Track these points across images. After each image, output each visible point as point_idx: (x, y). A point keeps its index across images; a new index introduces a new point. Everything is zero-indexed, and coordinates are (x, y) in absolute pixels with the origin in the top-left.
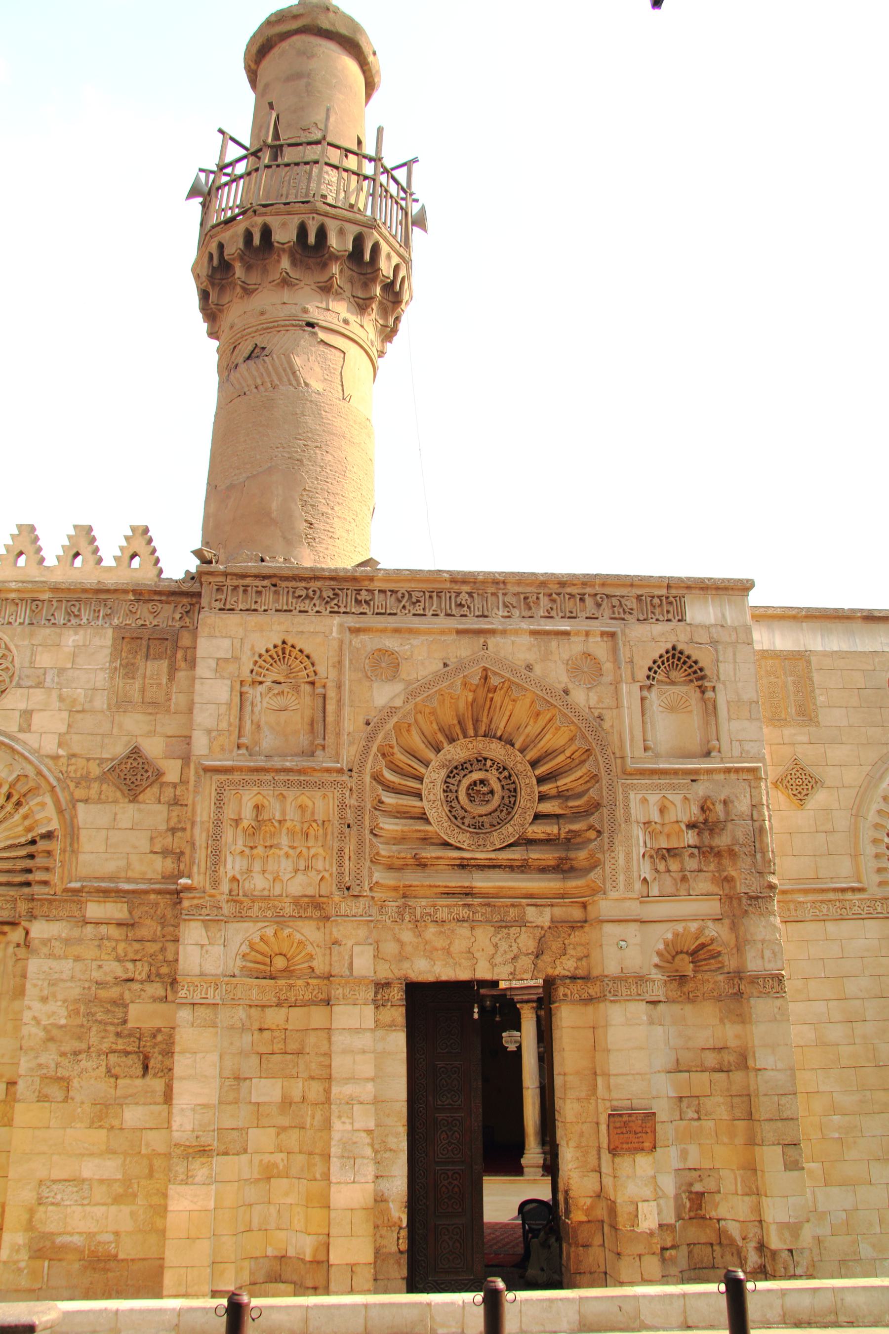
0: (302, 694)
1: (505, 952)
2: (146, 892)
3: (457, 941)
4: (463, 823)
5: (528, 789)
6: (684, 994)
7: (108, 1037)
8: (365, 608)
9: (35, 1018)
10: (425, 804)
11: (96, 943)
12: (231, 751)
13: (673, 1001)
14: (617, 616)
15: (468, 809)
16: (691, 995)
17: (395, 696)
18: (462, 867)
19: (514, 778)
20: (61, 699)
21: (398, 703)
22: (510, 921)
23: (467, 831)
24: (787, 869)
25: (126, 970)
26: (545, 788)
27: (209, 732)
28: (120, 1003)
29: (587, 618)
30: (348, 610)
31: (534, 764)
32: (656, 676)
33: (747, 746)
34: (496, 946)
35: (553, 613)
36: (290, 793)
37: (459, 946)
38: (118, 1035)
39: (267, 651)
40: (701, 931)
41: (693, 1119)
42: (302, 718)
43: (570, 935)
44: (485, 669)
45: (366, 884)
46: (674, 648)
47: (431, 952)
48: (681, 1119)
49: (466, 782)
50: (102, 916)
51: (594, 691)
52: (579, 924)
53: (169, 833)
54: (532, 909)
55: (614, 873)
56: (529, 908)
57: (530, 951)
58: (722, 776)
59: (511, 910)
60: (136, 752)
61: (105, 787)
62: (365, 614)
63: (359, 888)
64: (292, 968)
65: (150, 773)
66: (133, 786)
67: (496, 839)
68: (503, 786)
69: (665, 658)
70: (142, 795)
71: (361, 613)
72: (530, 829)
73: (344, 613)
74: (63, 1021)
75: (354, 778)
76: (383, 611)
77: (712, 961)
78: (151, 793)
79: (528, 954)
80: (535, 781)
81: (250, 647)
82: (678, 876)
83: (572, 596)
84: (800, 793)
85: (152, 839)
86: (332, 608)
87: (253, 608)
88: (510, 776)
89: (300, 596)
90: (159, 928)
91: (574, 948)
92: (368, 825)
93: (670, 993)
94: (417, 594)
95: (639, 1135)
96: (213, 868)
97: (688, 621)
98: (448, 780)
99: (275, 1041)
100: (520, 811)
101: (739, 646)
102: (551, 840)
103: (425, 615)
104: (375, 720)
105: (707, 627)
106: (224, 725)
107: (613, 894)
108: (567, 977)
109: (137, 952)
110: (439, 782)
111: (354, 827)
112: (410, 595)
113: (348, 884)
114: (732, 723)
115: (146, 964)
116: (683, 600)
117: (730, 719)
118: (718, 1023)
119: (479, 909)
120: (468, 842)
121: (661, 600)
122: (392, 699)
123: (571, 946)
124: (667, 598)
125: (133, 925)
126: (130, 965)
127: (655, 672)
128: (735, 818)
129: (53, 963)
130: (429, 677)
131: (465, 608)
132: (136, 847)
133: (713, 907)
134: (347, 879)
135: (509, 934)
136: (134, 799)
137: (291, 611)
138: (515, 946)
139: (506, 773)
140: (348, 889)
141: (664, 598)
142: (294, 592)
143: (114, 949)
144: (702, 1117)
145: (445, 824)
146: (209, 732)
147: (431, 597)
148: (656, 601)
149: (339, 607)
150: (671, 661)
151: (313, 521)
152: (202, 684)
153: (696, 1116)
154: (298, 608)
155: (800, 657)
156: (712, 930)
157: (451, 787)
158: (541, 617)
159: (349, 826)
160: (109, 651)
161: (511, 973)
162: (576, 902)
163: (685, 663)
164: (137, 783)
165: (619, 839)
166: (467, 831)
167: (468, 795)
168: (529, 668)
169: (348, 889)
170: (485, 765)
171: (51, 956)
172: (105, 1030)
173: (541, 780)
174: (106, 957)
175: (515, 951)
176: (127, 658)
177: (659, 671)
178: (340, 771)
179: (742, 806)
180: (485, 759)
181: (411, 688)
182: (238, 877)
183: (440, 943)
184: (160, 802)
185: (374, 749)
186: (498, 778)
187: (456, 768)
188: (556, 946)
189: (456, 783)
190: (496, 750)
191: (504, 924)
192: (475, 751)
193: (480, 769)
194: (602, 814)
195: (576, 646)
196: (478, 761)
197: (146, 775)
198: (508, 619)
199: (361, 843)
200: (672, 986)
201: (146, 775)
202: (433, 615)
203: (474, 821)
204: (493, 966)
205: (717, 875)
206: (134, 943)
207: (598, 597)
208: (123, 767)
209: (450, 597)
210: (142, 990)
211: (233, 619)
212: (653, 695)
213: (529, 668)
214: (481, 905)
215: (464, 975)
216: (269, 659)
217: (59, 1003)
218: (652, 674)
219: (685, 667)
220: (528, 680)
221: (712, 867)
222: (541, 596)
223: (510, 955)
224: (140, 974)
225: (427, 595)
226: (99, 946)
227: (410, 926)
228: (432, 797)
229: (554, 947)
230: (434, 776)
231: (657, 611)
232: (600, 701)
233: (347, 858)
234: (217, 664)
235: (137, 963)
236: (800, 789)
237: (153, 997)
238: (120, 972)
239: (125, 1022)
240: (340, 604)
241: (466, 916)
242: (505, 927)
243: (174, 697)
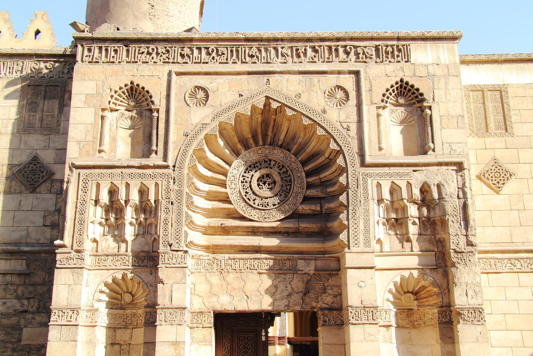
0: (144, 118)
2: (39, 252)
3: (249, 284)
4: (254, 203)
5: (300, 180)
6: (411, 322)
7: (6, 352)
8: (186, 59)
10: (228, 190)
11: (3, 287)
12: (94, 155)
13: (403, 327)
14: (361, 60)
15: (258, 193)
16: (416, 323)
17: (206, 117)
19: (290, 172)
21: (207, 121)
22: (286, 270)
23: (257, 209)
24: (484, 234)
25: (23, 305)
26: (311, 180)
27: (79, 142)
28: (17, 328)
29: (340, 62)
30: (175, 61)
31: (304, 163)
32: (389, 100)
33: (454, 147)
35: (316, 59)
36: (132, 182)
38: (14, 350)
39: (121, 88)
42: (144, 133)
43: (328, 280)
44: (267, 98)
45: (183, 241)
46: (402, 80)
50: (8, 268)
51: (343, 111)
52: (334, 272)
53: (56, 213)
54: (302, 261)
55: (356, 234)
56: (300, 261)
57: (300, 291)
58: (436, 168)
59: (287, 262)
60: (35, 159)
61: (13, 183)
62: (187, 63)
63: (177, 245)
64: (135, 302)
65: (44, 174)
66: (32, 182)
68: (282, 178)
69: (395, 88)
70: (38, 188)
71: (184, 63)
72: (300, 208)
73: (173, 63)
75: (176, 171)
76: (199, 61)
77: (431, 298)
78: (44, 187)
79: (299, 292)
81: (108, 87)
83: (330, 48)
84: (498, 183)
85: (45, 217)
86: (164, 59)
87: (111, 61)
88: (287, 171)
89: (143, 53)
90: (47, 276)
91: (332, 289)
92: (185, 203)
93: (400, 322)
94: (222, 49)
96: (79, 233)
97: (412, 62)
98: (245, 174)
99: (122, 352)
100: (294, 195)
101: (450, 78)
102: (316, 214)
103: (227, 63)
104: (192, 133)
105: (427, 66)
106: (90, 138)
107: (353, 249)
108: (325, 309)
109: (31, 293)
111: (176, 204)
112: (217, 51)
113: (170, 243)
114: (443, 130)
115: (37, 301)
116: (409, 47)
117: (442, 128)
118: (435, 343)
119: (265, 261)
120: (257, 215)
121: (393, 49)
122: (203, 119)
123: (329, 287)
124: (398, 46)
125: (29, 274)
126: (25, 302)
127: (388, 98)
130: (229, 104)
131: (255, 58)
132: (34, 223)
134: (170, 239)
135: (285, 279)
136: (33, 191)
137: (137, 62)
138: (289, 287)
139: (284, 170)
140: (170, 246)
141: (395, 47)
142: (139, 50)
143: (16, 291)
146: (79, 142)
147: (232, 51)
148: (390, 49)
149: (169, 59)
150: (399, 90)
151: (154, 4)
152: (75, 111)
154: (141, 60)
155: (501, 91)
157: (246, 179)
158: (308, 62)
159: (172, 204)
160: (19, 94)
161: (287, 306)
162: (333, 257)
163: (409, 90)
164: (35, 180)
165: (360, 211)
166: (257, 209)
167: (258, 185)
168: (299, 95)
169: (170, 246)
170: (270, 164)
172: (6, 347)
173: (309, 174)
174: (10, 297)
176: (31, 99)
177: (391, 97)
178: (167, 167)
179: (451, 189)
180: (270, 160)
181: (216, 112)
182: (98, 239)
183: (237, 284)
184: (51, 193)
185: (191, 152)
186: (279, 173)
188: (318, 286)
189: (250, 177)
190: (278, 154)
191: (282, 272)
192: (263, 155)
193: (267, 167)
194: (348, 194)
195: (332, 80)
196: (265, 162)
197: (42, 175)
198: (284, 64)
200: (402, 316)
201: (42, 175)
202: (233, 63)
203: (262, 201)
205: (433, 237)
206: (29, 286)
207: (348, 47)
208: (26, 169)
209: (245, 51)
210: (33, 318)
212: (385, 114)
213: (299, 95)
214: (266, 259)
216: (122, 94)
218: (385, 98)
219: (409, 94)
220: (297, 104)
221: (429, 232)
222: (308, 48)
223: (286, 293)
224: (32, 307)
225: (229, 50)
226: (5, 289)
228: (233, 186)
229: (317, 287)
230: (235, 172)
231: (390, 56)
232: (347, 117)
233: (170, 224)
234: (86, 98)
235: (31, 300)
236: (498, 180)
237: (40, 323)
238: (18, 307)
239: (20, 340)
240: (170, 57)
241: (256, 266)
242: (283, 274)
243: (62, 124)
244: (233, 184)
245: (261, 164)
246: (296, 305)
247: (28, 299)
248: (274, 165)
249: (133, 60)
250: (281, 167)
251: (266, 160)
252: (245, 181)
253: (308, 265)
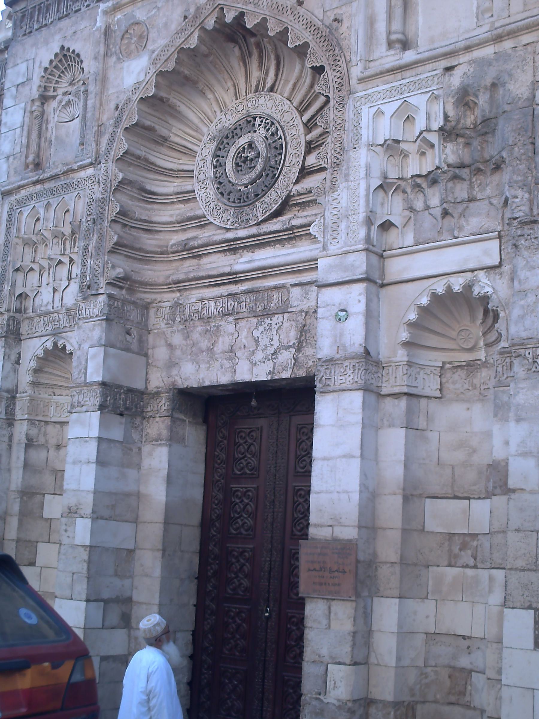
1: (266, 346)
16: (482, 388)
18: (234, 251)
19: (280, 133)
34: (257, 341)
40: (469, 287)
41: (467, 566)
47: (197, 355)
48: (450, 565)
49: (233, 150)
57: (291, 344)
67: (260, 211)
79: (289, 347)
82: (438, 212)
88: (277, 129)
95: (336, 574)
98: (219, 153)
106: (18, 149)
110: (209, 158)
119: (243, 298)
120: (232, 220)
128: (507, 108)
133: (488, 252)
134: (88, 279)
144: (479, 565)
145: (212, 205)
153: (471, 562)
156: (485, 285)
161: (270, 373)
186: (266, 137)
187: (227, 137)
193: (250, 132)
199: (101, 237)
200: (456, 377)
227: (182, 327)
228: (202, 177)
241: (230, 308)
244: (202, 173)
245: (241, 129)
246: (284, 369)
248: (260, 125)
249: (65, 13)
250: (270, 123)
251: (249, 119)
252: (218, 164)
253: (306, 296)
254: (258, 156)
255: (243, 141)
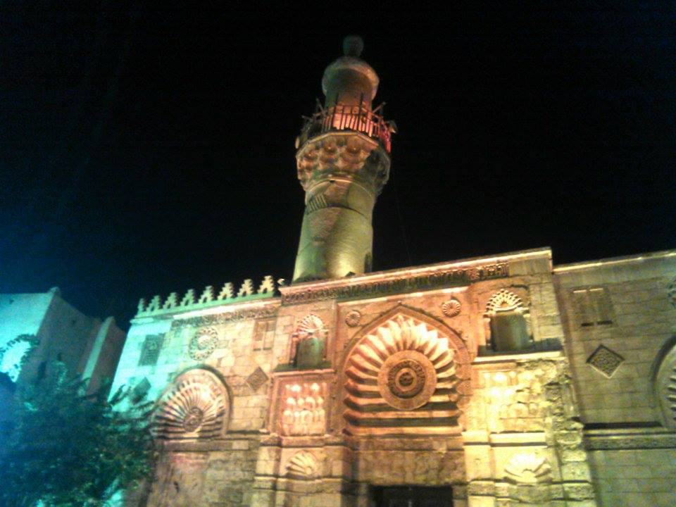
9: (207, 499)
19: (423, 370)
20: (233, 352)
34: (416, 464)
37: (397, 462)
49: (399, 374)
60: (259, 370)
68: (418, 376)
74: (217, 501)
79: (433, 469)
80: (434, 371)
85: (261, 411)
126: (246, 473)
129: (216, 472)
167: (400, 381)
171: (217, 469)
173: (438, 371)
175: (427, 466)
187: (394, 367)
204: (414, 475)
211: (292, 307)
215: (398, 480)
217: (217, 492)
223: (424, 470)
226: (235, 464)
238: (242, 477)
239: (241, 502)
246: (432, 480)
247: (248, 471)
253: (441, 445)
254: (412, 379)
255: (404, 370)
